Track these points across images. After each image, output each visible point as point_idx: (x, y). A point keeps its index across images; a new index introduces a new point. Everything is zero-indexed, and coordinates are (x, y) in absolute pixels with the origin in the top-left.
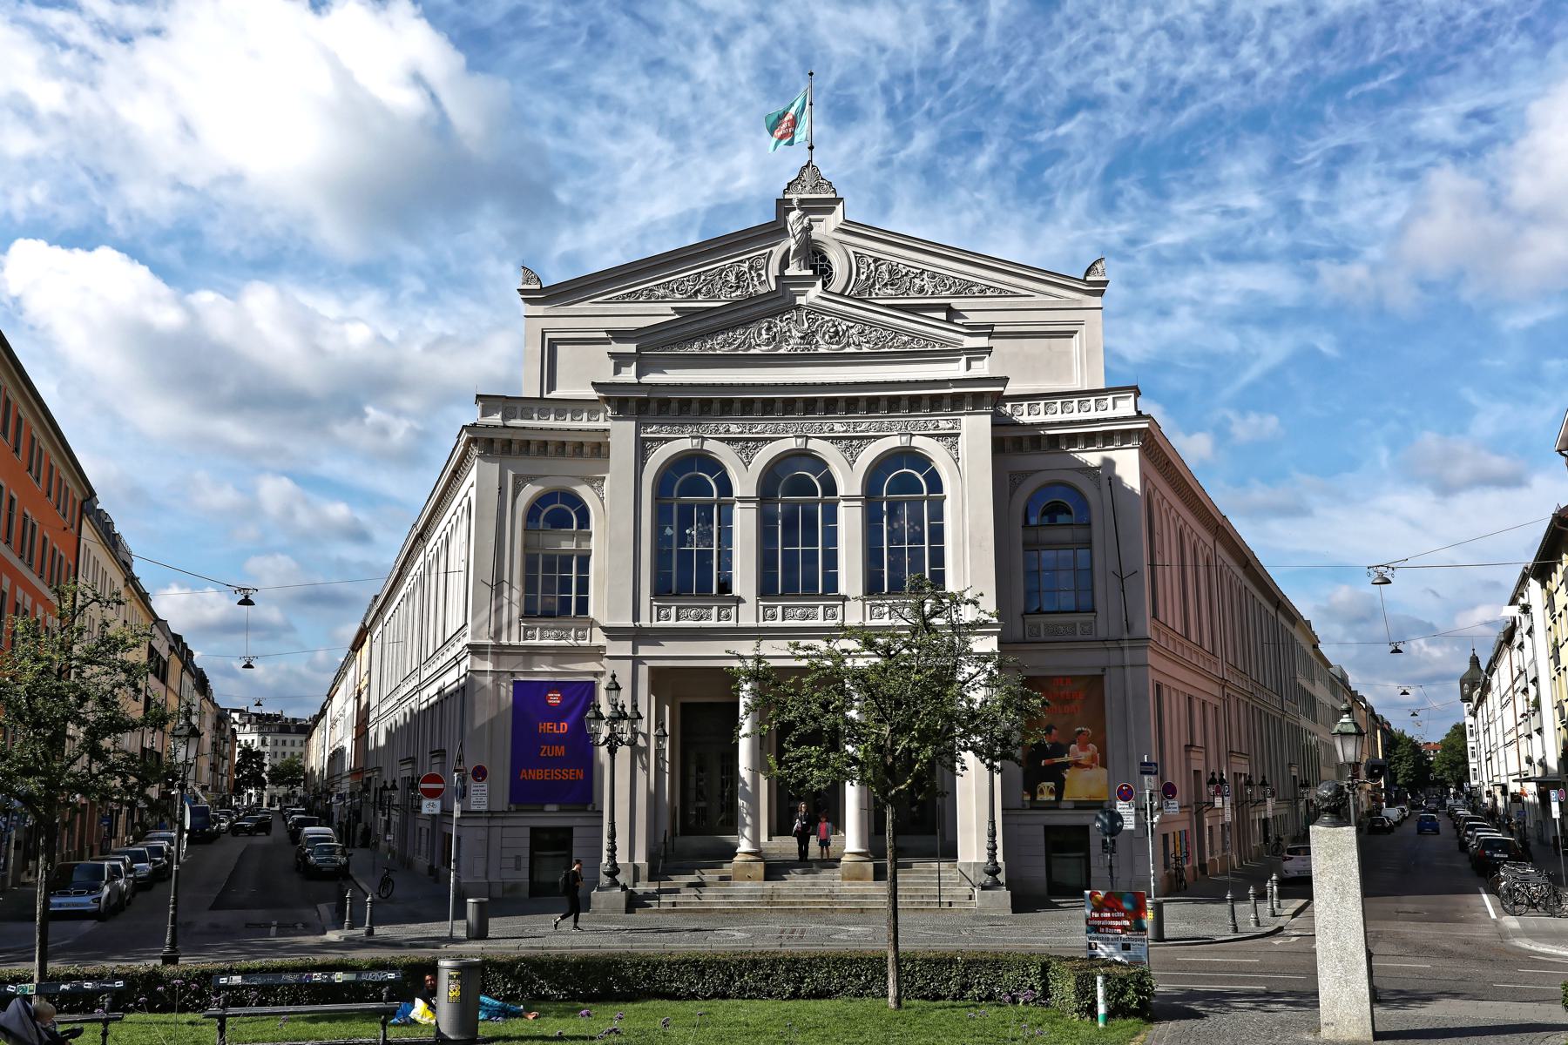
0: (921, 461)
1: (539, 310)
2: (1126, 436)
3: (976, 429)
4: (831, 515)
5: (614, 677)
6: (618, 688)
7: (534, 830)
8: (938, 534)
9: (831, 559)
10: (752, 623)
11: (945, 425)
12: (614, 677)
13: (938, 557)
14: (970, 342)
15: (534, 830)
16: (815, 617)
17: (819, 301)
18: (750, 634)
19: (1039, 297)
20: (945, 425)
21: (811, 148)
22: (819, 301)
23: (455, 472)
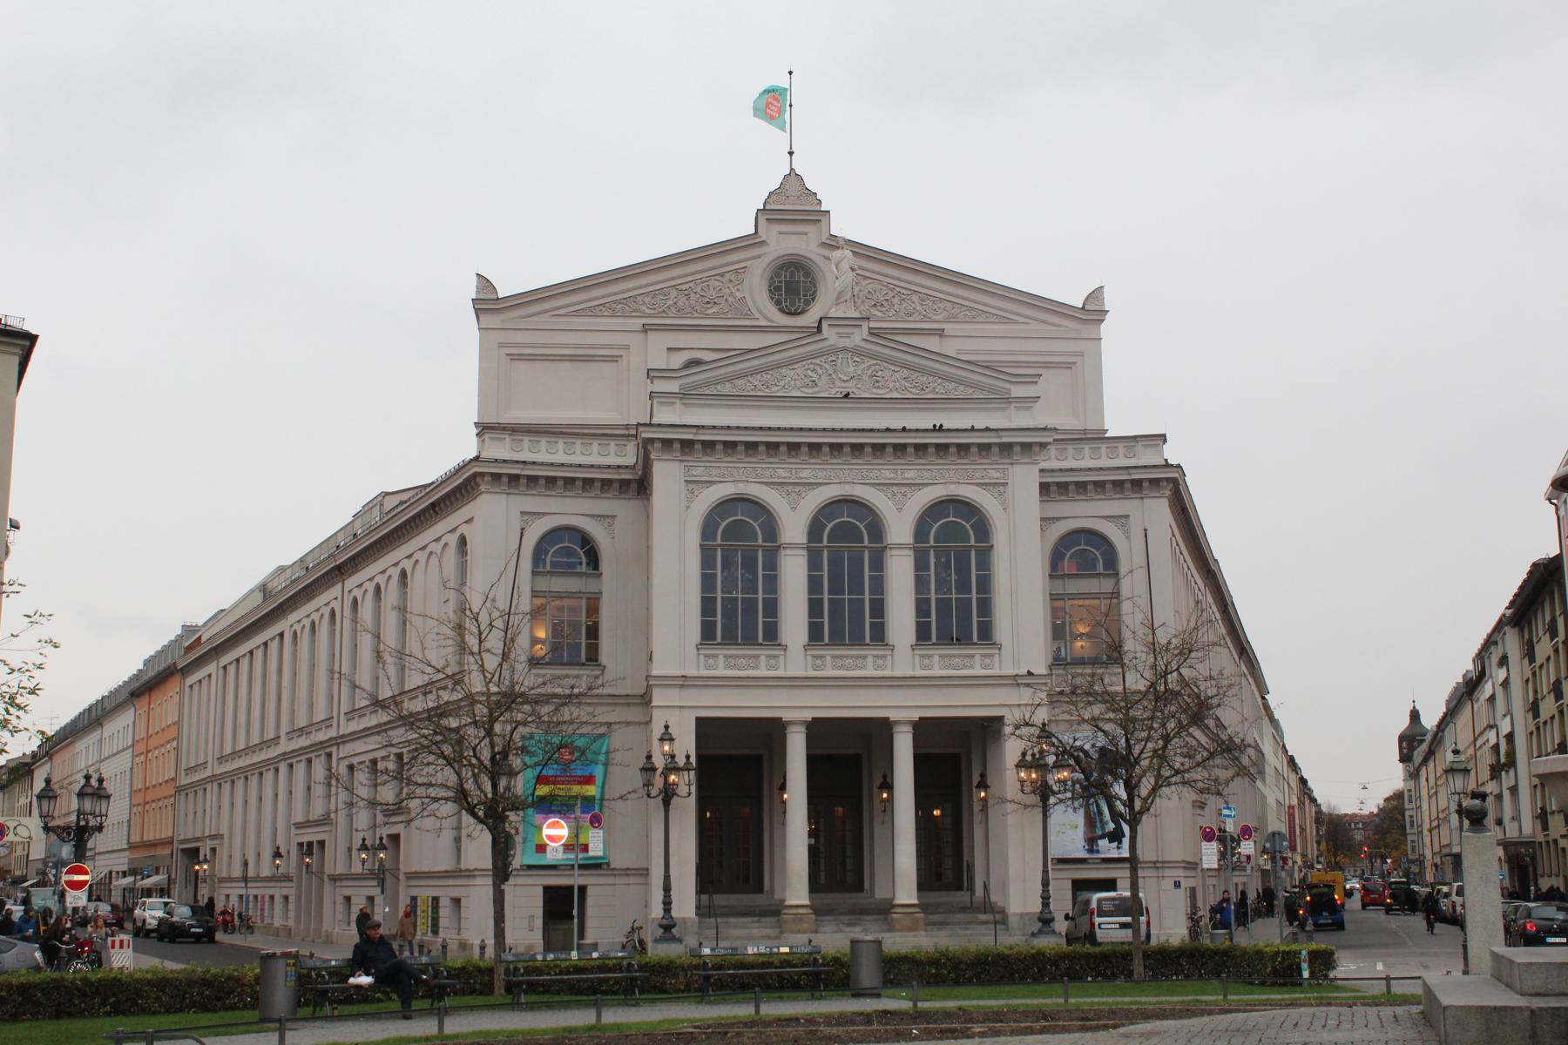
0: (967, 509)
1: (491, 321)
2: (1155, 482)
3: (1024, 478)
4: (878, 564)
5: (667, 727)
6: (672, 740)
7: (547, 889)
8: (985, 585)
9: (879, 608)
10: (802, 673)
11: (994, 475)
12: (667, 727)
13: (985, 607)
14: (1017, 391)
15: (547, 889)
16: (864, 668)
17: (864, 344)
18: (795, 684)
19: (1035, 326)
20: (994, 475)
21: (791, 153)
22: (864, 344)
23: (433, 505)
